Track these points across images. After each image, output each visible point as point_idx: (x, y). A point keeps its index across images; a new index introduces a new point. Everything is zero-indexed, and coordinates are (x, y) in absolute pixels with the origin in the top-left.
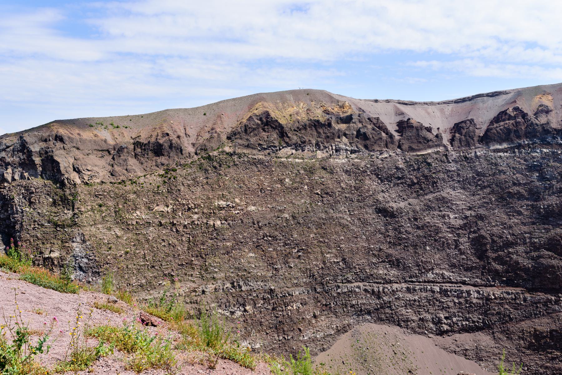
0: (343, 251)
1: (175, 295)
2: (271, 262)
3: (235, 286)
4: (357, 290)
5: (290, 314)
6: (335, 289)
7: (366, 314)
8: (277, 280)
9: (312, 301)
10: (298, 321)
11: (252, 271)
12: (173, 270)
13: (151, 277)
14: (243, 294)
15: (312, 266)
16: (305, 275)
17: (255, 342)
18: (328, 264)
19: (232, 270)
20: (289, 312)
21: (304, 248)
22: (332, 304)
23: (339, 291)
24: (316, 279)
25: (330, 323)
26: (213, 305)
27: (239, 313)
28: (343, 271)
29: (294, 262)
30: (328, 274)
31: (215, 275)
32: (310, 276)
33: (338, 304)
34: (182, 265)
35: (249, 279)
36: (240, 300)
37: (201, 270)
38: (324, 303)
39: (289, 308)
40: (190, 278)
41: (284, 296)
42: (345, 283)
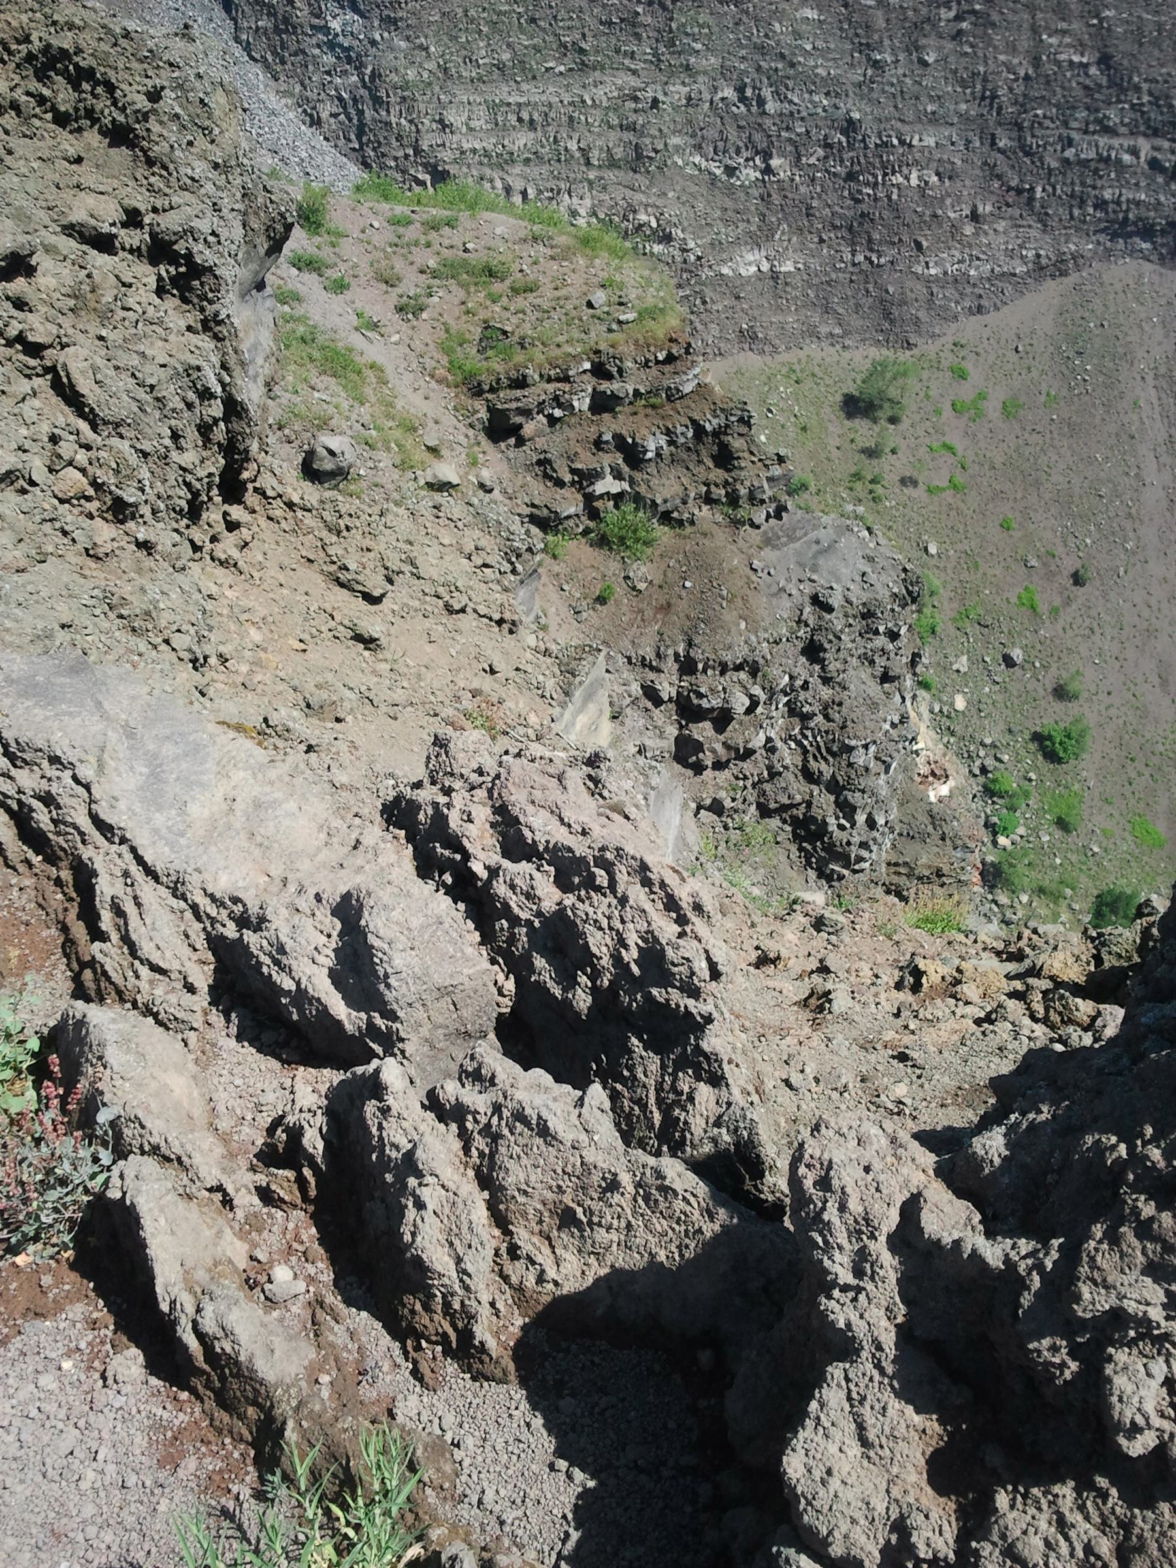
0: (1109, 29)
1: (583, 102)
2: (863, 41)
3: (747, 98)
4: (1127, 158)
5: (895, 197)
6: (1059, 148)
7: (1137, 233)
8: (875, 95)
9: (978, 172)
10: (917, 220)
11: (801, 59)
12: (584, 35)
13: (526, 47)
14: (768, 122)
15: (992, 67)
16: (968, 91)
17: (781, 256)
18: (1049, 69)
19: (744, 52)
20: (895, 191)
21: (977, 7)
22: (1039, 189)
23: (1070, 153)
24: (1000, 109)
25: (1019, 241)
26: (675, 140)
27: (750, 174)
28: (1097, 96)
29: (940, 49)
30: (1043, 97)
31: (692, 60)
32: (983, 98)
33: (1059, 191)
34: (610, 23)
35: (790, 83)
36: (757, 137)
37: (657, 41)
38: (1013, 183)
39: (898, 179)
40: (627, 62)
41: (885, 144)
42: (1094, 133)
